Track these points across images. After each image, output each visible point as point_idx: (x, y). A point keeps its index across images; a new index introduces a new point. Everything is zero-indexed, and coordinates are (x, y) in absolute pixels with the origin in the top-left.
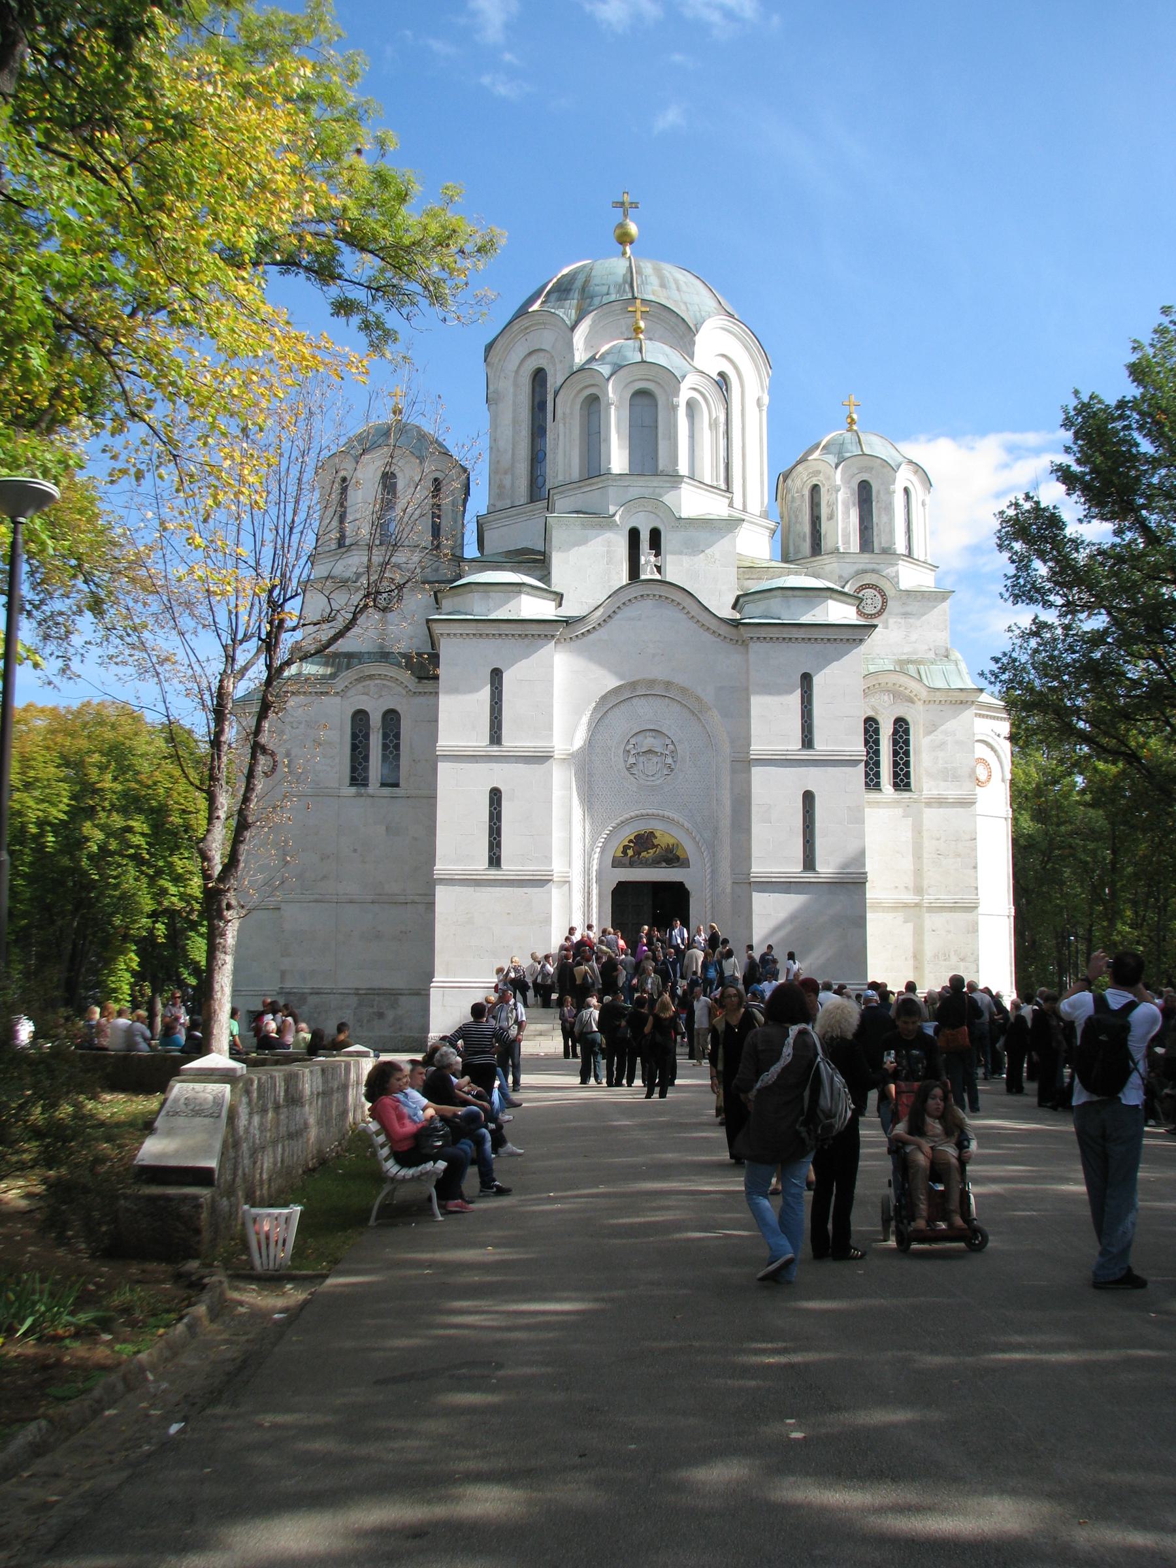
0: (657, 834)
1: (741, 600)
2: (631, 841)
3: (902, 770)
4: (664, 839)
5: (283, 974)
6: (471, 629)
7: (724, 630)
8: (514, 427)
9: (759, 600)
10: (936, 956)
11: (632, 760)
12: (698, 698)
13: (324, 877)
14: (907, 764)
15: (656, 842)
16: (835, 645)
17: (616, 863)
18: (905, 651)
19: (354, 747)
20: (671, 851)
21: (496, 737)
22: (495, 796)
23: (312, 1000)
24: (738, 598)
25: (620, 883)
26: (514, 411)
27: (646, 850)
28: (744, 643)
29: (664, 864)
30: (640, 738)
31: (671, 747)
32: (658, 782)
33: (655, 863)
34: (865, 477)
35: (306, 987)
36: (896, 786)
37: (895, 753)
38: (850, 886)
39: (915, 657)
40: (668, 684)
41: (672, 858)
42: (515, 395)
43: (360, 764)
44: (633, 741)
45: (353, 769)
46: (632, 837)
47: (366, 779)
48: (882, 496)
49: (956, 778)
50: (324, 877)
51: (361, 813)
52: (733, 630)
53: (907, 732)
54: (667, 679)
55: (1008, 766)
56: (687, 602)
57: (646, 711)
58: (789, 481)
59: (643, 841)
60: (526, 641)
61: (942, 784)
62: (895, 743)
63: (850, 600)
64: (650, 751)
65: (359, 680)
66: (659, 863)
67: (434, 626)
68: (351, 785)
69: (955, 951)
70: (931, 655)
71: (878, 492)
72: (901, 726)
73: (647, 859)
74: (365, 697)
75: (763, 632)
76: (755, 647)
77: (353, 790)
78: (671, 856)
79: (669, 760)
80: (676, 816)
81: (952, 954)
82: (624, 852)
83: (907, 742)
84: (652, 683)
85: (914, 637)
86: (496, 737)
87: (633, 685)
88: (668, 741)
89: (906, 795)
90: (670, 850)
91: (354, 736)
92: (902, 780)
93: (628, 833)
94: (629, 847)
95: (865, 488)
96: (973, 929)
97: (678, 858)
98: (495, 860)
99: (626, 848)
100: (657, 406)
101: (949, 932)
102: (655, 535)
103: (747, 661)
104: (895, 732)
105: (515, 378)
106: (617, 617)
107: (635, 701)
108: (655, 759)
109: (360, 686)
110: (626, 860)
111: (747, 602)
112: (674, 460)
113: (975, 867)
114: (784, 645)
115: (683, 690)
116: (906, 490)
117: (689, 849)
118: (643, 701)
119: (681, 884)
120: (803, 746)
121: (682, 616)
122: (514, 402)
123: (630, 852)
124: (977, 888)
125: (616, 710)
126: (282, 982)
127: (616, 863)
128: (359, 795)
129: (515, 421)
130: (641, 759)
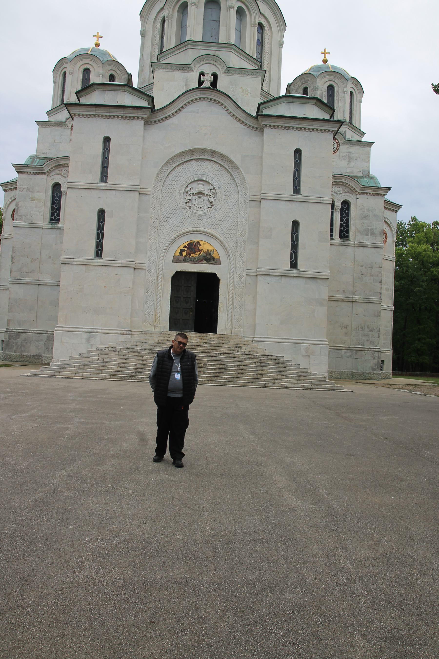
0: (202, 243)
1: (261, 107)
2: (185, 247)
3: (344, 229)
4: (205, 247)
5: (9, 321)
6: (92, 111)
7: (249, 121)
8: (152, 47)
9: (272, 106)
10: (357, 328)
11: (189, 198)
12: (231, 162)
13: (33, 271)
14: (347, 226)
15: (200, 248)
16: (316, 133)
17: (176, 260)
18: (347, 171)
19: (53, 203)
20: (210, 254)
21: (104, 178)
22: (102, 213)
23: (23, 336)
24: (260, 105)
25: (177, 273)
26: (152, 39)
27: (194, 252)
28: (261, 130)
29: (205, 262)
30: (194, 185)
31: (214, 191)
32: (204, 211)
33: (199, 261)
34: (332, 83)
35: (20, 329)
36: (341, 237)
37: (341, 220)
38: (319, 281)
39: (352, 175)
40: (213, 153)
41: (209, 258)
42: (153, 31)
43: (56, 212)
44: (189, 186)
45: (52, 214)
46: (186, 244)
47: (58, 220)
48: (341, 94)
49: (373, 234)
50: (33, 271)
51: (50, 236)
52: (255, 121)
53: (348, 209)
54: (213, 149)
55: (395, 235)
56: (227, 103)
57: (200, 169)
58: (292, 86)
59: (193, 247)
60: (126, 121)
61: (365, 237)
62: (342, 214)
63: (327, 109)
64: (200, 193)
65: (57, 167)
66: (202, 260)
67: (69, 108)
68: (50, 222)
69: (368, 326)
70: (361, 175)
71: (338, 91)
72: (345, 206)
73: (195, 258)
74: (60, 176)
75: (274, 122)
76: (267, 131)
77: (50, 225)
78: (209, 257)
79: (212, 199)
80: (212, 232)
81: (366, 327)
82: (181, 253)
83: (348, 215)
84: (203, 151)
85: (352, 164)
86: (104, 178)
87: (192, 152)
88: (212, 188)
89: (346, 242)
90: (209, 253)
91: (53, 197)
92: (344, 234)
93: (184, 242)
94: (184, 250)
95: (330, 89)
96: (378, 315)
97: (213, 259)
98: (99, 254)
99: (182, 251)
100: (220, 9)
101: (365, 316)
102: (215, 76)
103: (263, 141)
104: (342, 209)
105: (154, 22)
106: (184, 110)
107: (192, 162)
108: (204, 198)
109: (57, 171)
110: (182, 258)
111: (265, 108)
112: (229, 37)
113: (380, 282)
114: (285, 131)
115: (222, 156)
116: (351, 93)
117: (220, 253)
118: (197, 162)
119: (214, 275)
120: (294, 193)
121: (224, 112)
122: (153, 35)
123: (184, 254)
124: (381, 293)
125: (181, 167)
126: (8, 326)
127: (176, 260)
128: (52, 228)
129: (153, 45)
130: (194, 197)
